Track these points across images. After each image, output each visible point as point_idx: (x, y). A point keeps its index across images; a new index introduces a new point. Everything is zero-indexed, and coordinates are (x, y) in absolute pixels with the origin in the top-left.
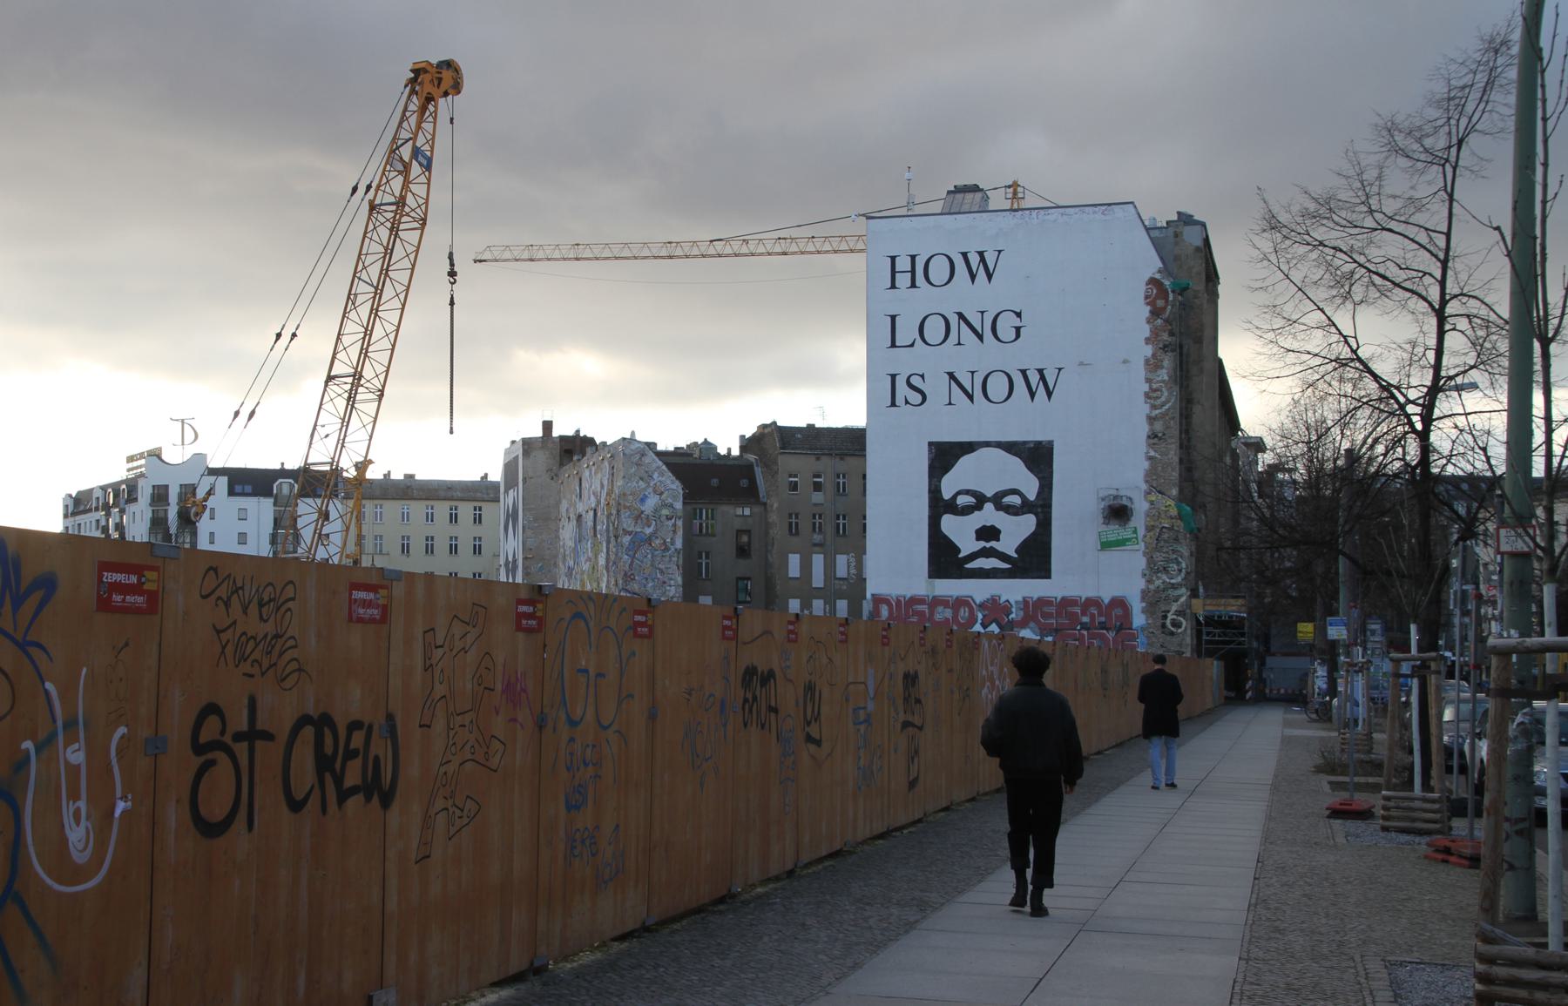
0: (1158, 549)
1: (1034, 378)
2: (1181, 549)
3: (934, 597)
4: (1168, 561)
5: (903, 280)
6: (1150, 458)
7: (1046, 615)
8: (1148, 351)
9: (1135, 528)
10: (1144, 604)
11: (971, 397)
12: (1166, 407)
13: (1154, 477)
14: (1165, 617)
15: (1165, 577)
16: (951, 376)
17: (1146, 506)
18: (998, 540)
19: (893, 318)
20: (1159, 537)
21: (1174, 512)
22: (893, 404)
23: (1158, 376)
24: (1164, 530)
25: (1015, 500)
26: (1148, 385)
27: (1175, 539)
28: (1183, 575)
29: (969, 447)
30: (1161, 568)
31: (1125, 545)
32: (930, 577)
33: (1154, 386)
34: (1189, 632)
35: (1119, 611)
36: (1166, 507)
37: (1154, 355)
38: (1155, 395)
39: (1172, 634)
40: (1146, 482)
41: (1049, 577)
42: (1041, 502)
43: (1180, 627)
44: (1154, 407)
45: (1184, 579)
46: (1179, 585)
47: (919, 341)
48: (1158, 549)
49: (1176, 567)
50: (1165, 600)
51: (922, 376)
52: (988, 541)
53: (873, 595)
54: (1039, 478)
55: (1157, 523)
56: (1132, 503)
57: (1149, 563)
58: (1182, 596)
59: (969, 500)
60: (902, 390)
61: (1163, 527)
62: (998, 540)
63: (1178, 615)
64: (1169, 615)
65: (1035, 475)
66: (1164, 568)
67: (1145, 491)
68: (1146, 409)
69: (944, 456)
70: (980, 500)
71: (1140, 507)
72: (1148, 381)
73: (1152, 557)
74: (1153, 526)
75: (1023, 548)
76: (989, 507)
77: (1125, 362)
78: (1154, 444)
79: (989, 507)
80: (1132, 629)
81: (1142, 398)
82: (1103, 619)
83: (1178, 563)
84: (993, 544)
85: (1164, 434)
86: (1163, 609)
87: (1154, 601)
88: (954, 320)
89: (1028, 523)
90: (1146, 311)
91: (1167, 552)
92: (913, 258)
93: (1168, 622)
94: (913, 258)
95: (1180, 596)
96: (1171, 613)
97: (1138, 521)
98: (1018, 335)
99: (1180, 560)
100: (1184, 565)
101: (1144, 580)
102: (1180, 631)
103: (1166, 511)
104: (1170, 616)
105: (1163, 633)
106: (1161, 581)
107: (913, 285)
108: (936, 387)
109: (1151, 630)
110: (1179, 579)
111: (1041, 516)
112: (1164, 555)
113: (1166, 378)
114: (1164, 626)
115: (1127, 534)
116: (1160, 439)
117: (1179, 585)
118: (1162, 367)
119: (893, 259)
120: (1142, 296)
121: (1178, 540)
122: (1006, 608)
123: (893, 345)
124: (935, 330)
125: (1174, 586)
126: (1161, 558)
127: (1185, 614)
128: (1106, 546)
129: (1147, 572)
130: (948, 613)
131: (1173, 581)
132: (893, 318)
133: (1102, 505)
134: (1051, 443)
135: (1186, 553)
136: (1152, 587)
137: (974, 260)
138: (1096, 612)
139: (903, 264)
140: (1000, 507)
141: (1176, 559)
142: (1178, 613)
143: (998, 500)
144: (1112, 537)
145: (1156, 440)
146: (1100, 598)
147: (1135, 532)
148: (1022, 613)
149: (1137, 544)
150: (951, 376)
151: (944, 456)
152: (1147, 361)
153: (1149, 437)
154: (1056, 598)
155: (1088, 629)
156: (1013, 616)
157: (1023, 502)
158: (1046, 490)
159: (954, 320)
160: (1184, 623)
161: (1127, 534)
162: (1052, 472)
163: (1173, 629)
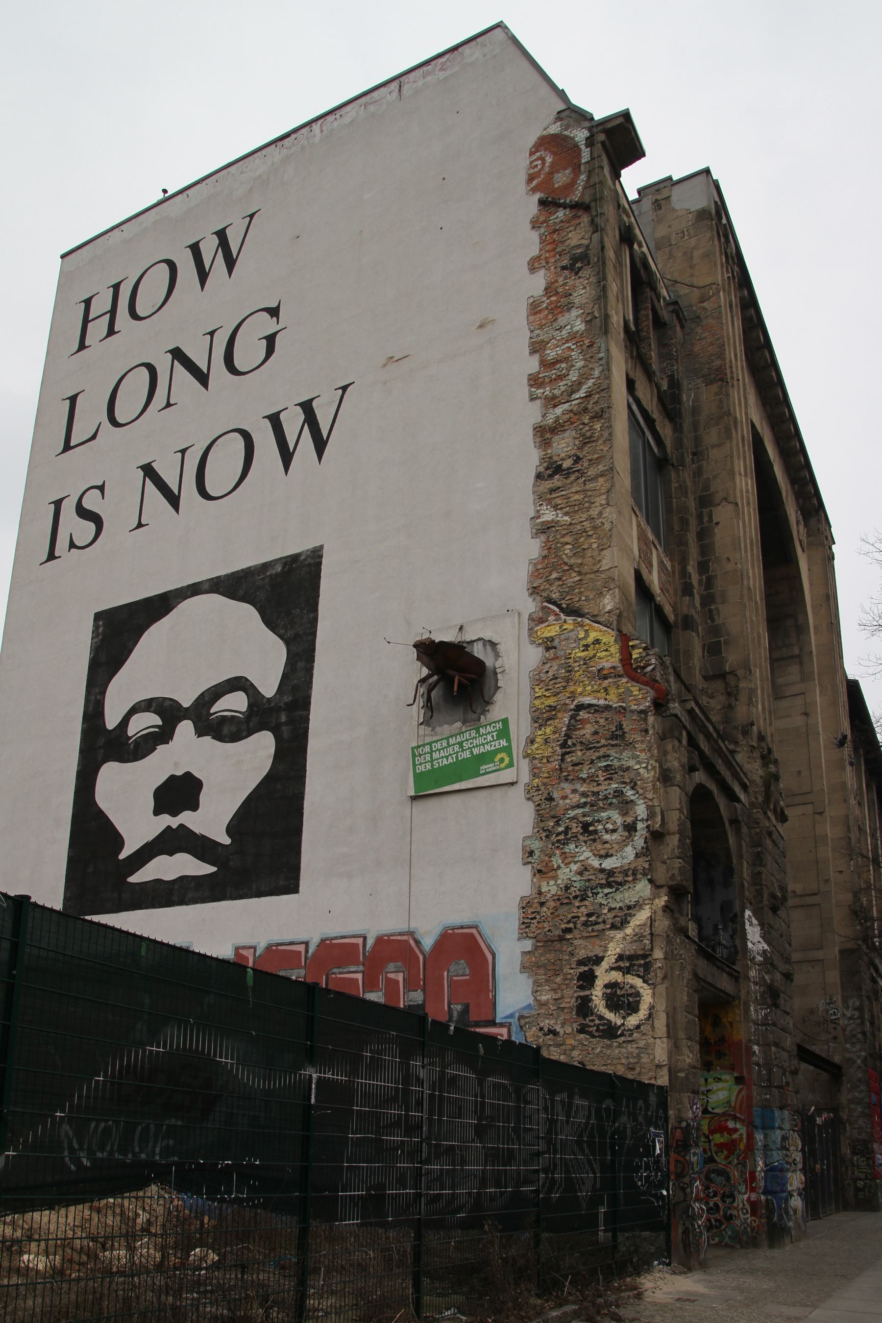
0: (563, 774)
2: (631, 763)
4: (595, 802)
6: (544, 529)
8: (538, 283)
9: (505, 722)
10: (528, 945)
12: (582, 393)
13: (554, 575)
14: (588, 979)
15: (585, 854)
16: (149, 471)
17: (534, 655)
18: (194, 806)
20: (568, 736)
21: (610, 658)
23: (561, 329)
24: (583, 714)
26: (536, 358)
27: (614, 737)
28: (639, 841)
30: (576, 828)
31: (478, 774)
33: (551, 354)
34: (661, 1022)
36: (587, 646)
37: (549, 290)
38: (553, 373)
39: (610, 1032)
40: (534, 591)
42: (287, 699)
43: (633, 1008)
44: (552, 402)
46: (631, 874)
48: (563, 774)
49: (616, 816)
50: (585, 924)
52: (174, 814)
54: (287, 642)
55: (563, 697)
56: (497, 655)
57: (541, 817)
58: (637, 906)
59: (151, 720)
60: (70, 521)
61: (580, 707)
63: (626, 971)
64: (599, 971)
65: (281, 637)
66: (585, 827)
67: (531, 618)
68: (533, 413)
72: (536, 347)
73: (550, 799)
74: (552, 708)
76: (185, 729)
78: (552, 491)
79: (185, 729)
80: (493, 1023)
81: (524, 391)
83: (626, 806)
84: (186, 818)
85: (578, 459)
86: (582, 954)
90: (531, 205)
91: (592, 779)
93: (597, 994)
95: (631, 908)
96: (605, 965)
99: (629, 793)
100: (641, 810)
101: (527, 871)
102: (633, 1021)
103: (586, 661)
104: (604, 976)
105: (582, 1030)
106: (574, 867)
109: (546, 1023)
110: (629, 853)
111: (286, 731)
112: (583, 788)
113: (580, 326)
114: (584, 1007)
116: (568, 473)
117: (631, 874)
118: (569, 307)
120: (523, 177)
121: (623, 736)
126: (575, 799)
127: (647, 967)
129: (536, 845)
131: (608, 864)
135: (646, 772)
136: (551, 888)
138: (400, 977)
141: (619, 793)
144: (444, 757)
145: (557, 481)
146: (411, 933)
147: (504, 733)
149: (511, 765)
152: (534, 308)
153: (539, 476)
154: (307, 944)
157: (250, 706)
158: (301, 665)
160: (647, 997)
162: (316, 619)
163: (610, 1016)
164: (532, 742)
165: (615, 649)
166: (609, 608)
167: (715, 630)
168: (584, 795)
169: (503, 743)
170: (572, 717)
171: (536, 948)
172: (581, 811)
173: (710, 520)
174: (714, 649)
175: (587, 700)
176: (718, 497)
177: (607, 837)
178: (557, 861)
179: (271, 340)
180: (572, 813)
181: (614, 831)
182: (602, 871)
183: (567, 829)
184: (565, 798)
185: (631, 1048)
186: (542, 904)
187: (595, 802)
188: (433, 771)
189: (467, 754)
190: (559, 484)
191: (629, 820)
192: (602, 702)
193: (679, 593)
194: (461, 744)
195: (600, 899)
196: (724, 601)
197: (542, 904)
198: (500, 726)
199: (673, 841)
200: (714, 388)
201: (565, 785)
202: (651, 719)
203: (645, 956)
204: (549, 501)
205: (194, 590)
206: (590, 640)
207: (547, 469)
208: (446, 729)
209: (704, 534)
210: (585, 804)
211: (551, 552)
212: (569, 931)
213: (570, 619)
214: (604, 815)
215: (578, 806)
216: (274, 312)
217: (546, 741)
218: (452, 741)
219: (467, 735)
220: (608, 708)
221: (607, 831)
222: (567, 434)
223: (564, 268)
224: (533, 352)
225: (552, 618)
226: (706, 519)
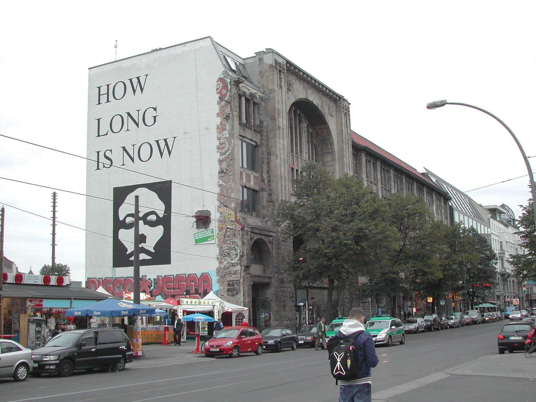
2: (237, 241)
6: (220, 186)
9: (213, 229)
10: (218, 277)
12: (228, 153)
15: (228, 259)
23: (223, 135)
27: (233, 235)
33: (222, 141)
40: (218, 200)
44: (222, 154)
50: (228, 274)
61: (227, 228)
68: (217, 156)
72: (219, 138)
73: (222, 247)
74: (222, 228)
83: (236, 250)
85: (227, 170)
91: (229, 244)
100: (239, 251)
106: (226, 262)
131: (233, 262)
136: (222, 266)
141: (234, 247)
145: (223, 175)
147: (212, 232)
164: (218, 235)
165: (234, 216)
166: (233, 207)
167: (270, 190)
168: (228, 247)
169: (212, 234)
170: (226, 230)
171: (220, 278)
172: (227, 250)
173: (270, 159)
174: (270, 195)
175: (229, 227)
176: (272, 153)
177: (232, 256)
178: (223, 260)
180: (226, 251)
181: (234, 255)
182: (231, 263)
183: (225, 254)
184: (224, 247)
185: (237, 298)
186: (221, 269)
188: (199, 239)
189: (205, 236)
190: (223, 175)
191: (236, 253)
192: (231, 227)
193: (261, 181)
194: (204, 233)
195: (231, 269)
196: (273, 182)
197: (221, 269)
198: (212, 230)
199: (245, 257)
200: (272, 121)
201: (224, 244)
202: (240, 232)
203: (239, 281)
204: (221, 179)
206: (229, 213)
207: (221, 171)
208: (201, 230)
209: (268, 163)
210: (228, 249)
211: (222, 190)
212: (226, 275)
213: (225, 208)
214: (232, 251)
215: (227, 249)
217: (221, 235)
218: (202, 233)
219: (205, 232)
220: (232, 229)
221: (232, 255)
222: (225, 163)
223: (224, 118)
224: (218, 139)
225: (222, 207)
226: (269, 159)
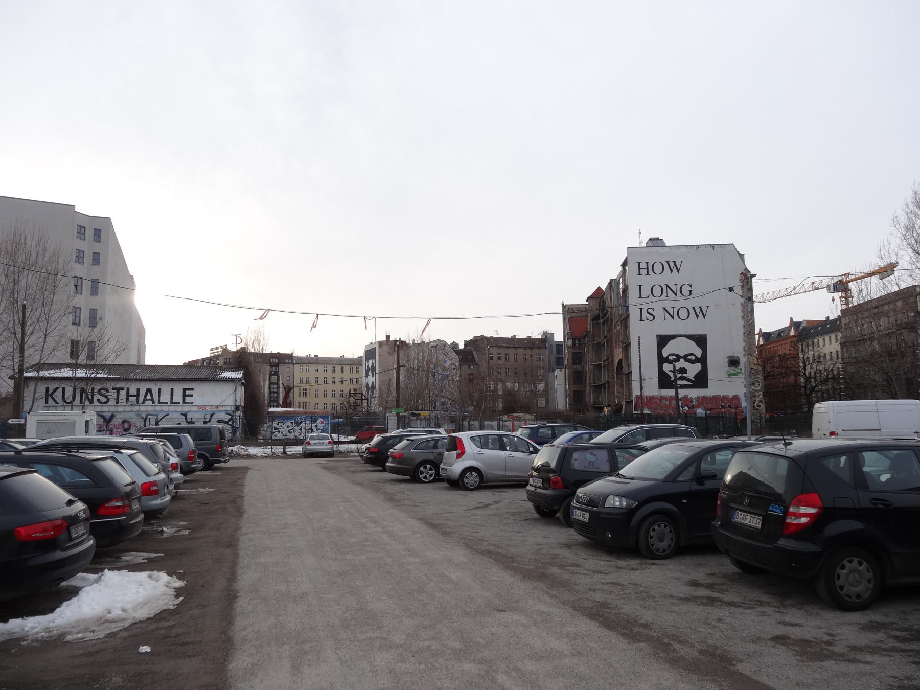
1: (698, 310)
3: (661, 396)
5: (644, 272)
7: (707, 403)
11: (673, 317)
16: (665, 309)
19: (640, 286)
22: (642, 320)
25: (693, 358)
28: (760, 386)
29: (673, 337)
32: (659, 388)
35: (736, 401)
41: (708, 388)
43: (760, 407)
45: (761, 388)
46: (759, 391)
47: (651, 295)
51: (653, 309)
53: (636, 395)
60: (645, 314)
62: (686, 373)
69: (663, 341)
70: (678, 357)
71: (743, 360)
75: (696, 377)
76: (682, 360)
77: (733, 304)
79: (682, 360)
82: (730, 404)
83: (759, 382)
84: (684, 375)
87: (751, 396)
88: (665, 287)
89: (698, 367)
92: (647, 263)
93: (756, 406)
94: (647, 263)
95: (759, 395)
97: (742, 365)
98: (690, 294)
104: (756, 403)
107: (648, 274)
108: (659, 313)
114: (754, 406)
115: (738, 371)
117: (759, 391)
119: (639, 263)
122: (691, 400)
123: (641, 297)
124: (657, 291)
125: (757, 391)
128: (730, 375)
130: (667, 403)
132: (640, 286)
133: (727, 359)
134: (706, 335)
135: (761, 378)
137: (672, 264)
139: (643, 265)
140: (686, 360)
142: (759, 401)
143: (685, 357)
144: (732, 372)
147: (741, 370)
148: (697, 402)
150: (665, 309)
151: (663, 341)
155: (724, 408)
156: (694, 403)
159: (665, 287)
161: (738, 371)
179: (690, 291)
187: (754, 381)
205: (680, 336)
208: (732, 368)
216: (690, 286)
